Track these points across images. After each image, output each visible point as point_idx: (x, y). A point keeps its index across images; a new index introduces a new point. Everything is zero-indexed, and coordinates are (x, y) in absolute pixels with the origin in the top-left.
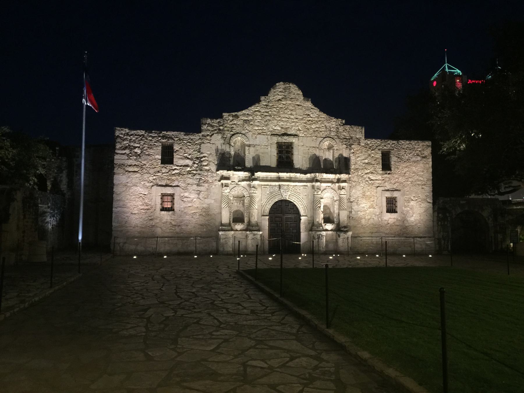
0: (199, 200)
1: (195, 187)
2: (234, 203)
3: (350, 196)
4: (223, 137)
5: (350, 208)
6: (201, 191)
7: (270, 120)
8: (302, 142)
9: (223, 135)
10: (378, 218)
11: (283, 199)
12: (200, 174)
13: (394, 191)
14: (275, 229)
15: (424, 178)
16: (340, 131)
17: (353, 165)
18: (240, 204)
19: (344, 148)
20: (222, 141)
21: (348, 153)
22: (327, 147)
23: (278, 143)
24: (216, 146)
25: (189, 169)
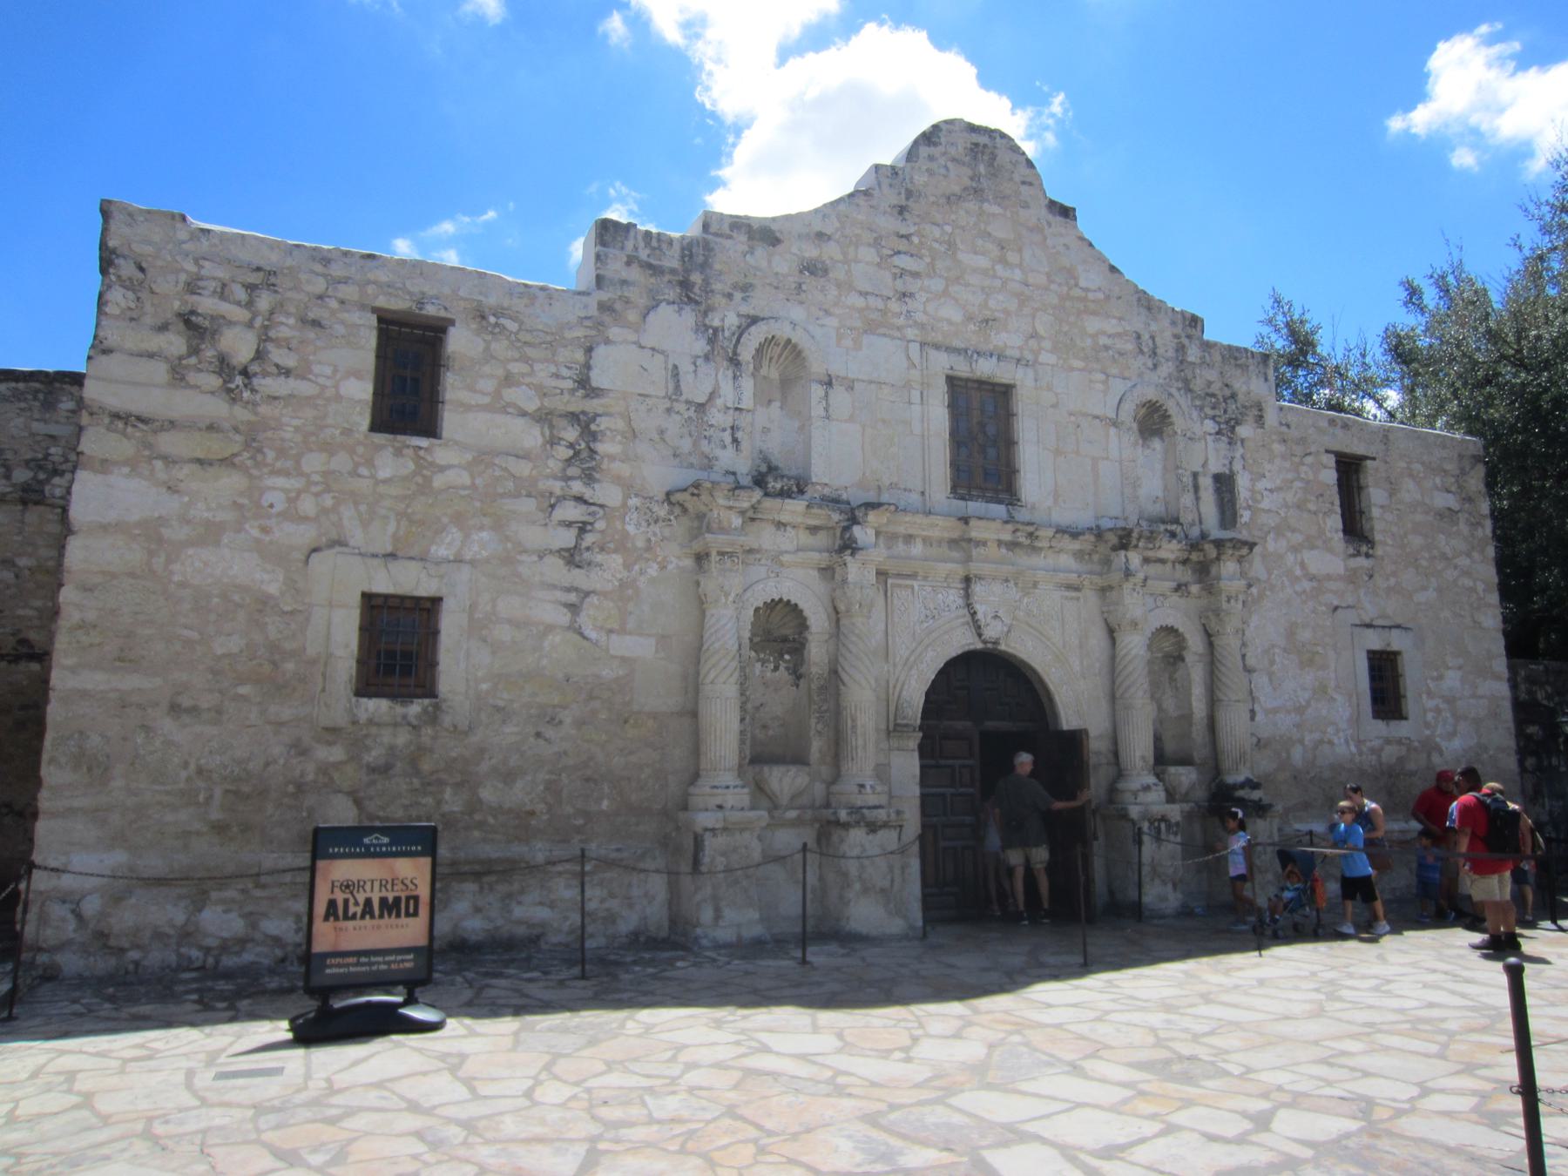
0: (578, 638)
1: (555, 569)
4: (702, 328)
6: (587, 594)
8: (1049, 388)
9: (705, 314)
10: (1347, 742)
11: (980, 646)
12: (586, 502)
13: (1390, 627)
14: (943, 795)
16: (1190, 359)
17: (1245, 509)
18: (776, 668)
20: (701, 346)
23: (952, 381)
24: (670, 367)
25: (524, 469)
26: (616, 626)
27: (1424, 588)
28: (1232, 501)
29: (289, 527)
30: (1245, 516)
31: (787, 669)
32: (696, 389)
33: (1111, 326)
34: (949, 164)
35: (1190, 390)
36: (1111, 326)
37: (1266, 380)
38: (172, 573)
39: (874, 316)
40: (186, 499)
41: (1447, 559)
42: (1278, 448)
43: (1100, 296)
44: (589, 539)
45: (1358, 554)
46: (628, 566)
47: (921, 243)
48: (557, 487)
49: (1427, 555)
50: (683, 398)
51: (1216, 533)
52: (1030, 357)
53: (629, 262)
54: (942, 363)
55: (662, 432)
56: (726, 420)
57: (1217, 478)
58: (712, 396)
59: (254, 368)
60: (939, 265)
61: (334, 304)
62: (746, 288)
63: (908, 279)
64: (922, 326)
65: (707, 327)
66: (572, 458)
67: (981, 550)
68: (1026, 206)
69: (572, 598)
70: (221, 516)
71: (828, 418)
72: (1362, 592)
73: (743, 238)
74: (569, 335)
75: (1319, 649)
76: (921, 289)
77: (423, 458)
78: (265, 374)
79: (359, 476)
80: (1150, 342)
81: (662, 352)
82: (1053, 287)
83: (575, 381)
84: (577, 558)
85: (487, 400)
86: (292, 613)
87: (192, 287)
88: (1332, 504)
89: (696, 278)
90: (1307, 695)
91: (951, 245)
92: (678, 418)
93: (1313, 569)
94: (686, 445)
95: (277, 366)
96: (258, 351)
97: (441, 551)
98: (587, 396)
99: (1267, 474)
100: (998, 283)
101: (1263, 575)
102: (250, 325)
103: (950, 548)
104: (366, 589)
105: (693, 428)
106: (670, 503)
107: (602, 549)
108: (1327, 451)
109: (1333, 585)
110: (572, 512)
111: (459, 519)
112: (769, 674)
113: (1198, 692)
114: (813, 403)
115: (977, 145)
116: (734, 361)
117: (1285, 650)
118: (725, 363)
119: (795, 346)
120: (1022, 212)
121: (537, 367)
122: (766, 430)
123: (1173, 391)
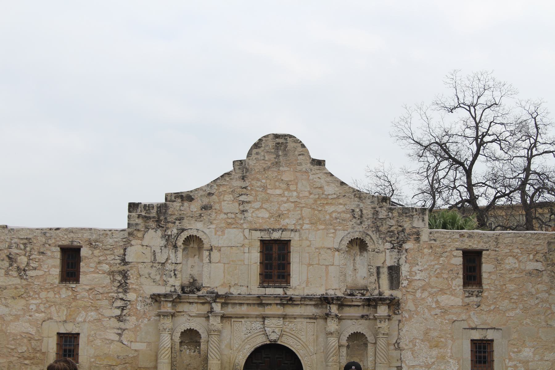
1: (114, 323)
2: (184, 351)
3: (399, 338)
4: (163, 236)
5: (398, 360)
6: (124, 330)
7: (248, 202)
8: (307, 239)
9: (165, 231)
11: (268, 342)
12: (124, 300)
15: (550, 305)
16: (380, 217)
17: (405, 280)
18: (195, 352)
19: (388, 249)
20: (163, 242)
21: (395, 258)
22: (358, 247)
23: (263, 242)
24: (152, 251)
26: (133, 340)
27: (513, 309)
28: (398, 277)
29: (37, 315)
30: (405, 283)
31: (198, 351)
32: (161, 258)
33: (341, 208)
34: (265, 154)
35: (379, 231)
36: (341, 208)
37: (423, 220)
38: (7, 330)
39: (229, 221)
40: (10, 309)
41: (532, 295)
42: (426, 251)
43: (335, 196)
44: (125, 312)
45: (471, 294)
46: (137, 320)
47: (251, 189)
48: (115, 295)
49: (517, 294)
50: (157, 261)
51: (387, 293)
52: (298, 227)
53: (139, 216)
54: (258, 235)
55: (149, 274)
56: (172, 267)
57: (390, 268)
58: (167, 259)
59: (27, 268)
60: (260, 196)
61: (47, 246)
62: (180, 219)
63: (246, 205)
64: (251, 222)
65: (166, 235)
66: (120, 286)
67: (269, 307)
68: (300, 164)
69: (120, 332)
70: (19, 313)
71: (210, 262)
72: (472, 313)
73: (179, 200)
74: (118, 244)
75: (442, 340)
76: (250, 208)
77: (74, 290)
78: (30, 270)
79: (56, 298)
80: (360, 213)
81: (150, 247)
82: (311, 196)
83: (121, 260)
84: (121, 319)
85: (93, 269)
86: (39, 340)
87: (10, 247)
88: (458, 274)
89: (162, 218)
90: (433, 360)
91: (265, 188)
92: (155, 268)
93: (442, 304)
94: (158, 277)
95: (32, 267)
96: (27, 263)
97: (80, 319)
98: (124, 265)
99: (419, 263)
100: (285, 199)
101: (413, 308)
102: (25, 255)
103: (258, 307)
104: (58, 331)
105: (160, 272)
106: (152, 298)
107: (129, 315)
108: (457, 249)
109: (454, 311)
110: (119, 303)
111: (85, 308)
112: (192, 353)
113: (371, 359)
114: (204, 258)
115: (278, 143)
116: (175, 247)
117: (422, 340)
118: (172, 248)
119: (199, 237)
120: (299, 168)
121: (108, 257)
122: (192, 267)
123: (370, 233)
